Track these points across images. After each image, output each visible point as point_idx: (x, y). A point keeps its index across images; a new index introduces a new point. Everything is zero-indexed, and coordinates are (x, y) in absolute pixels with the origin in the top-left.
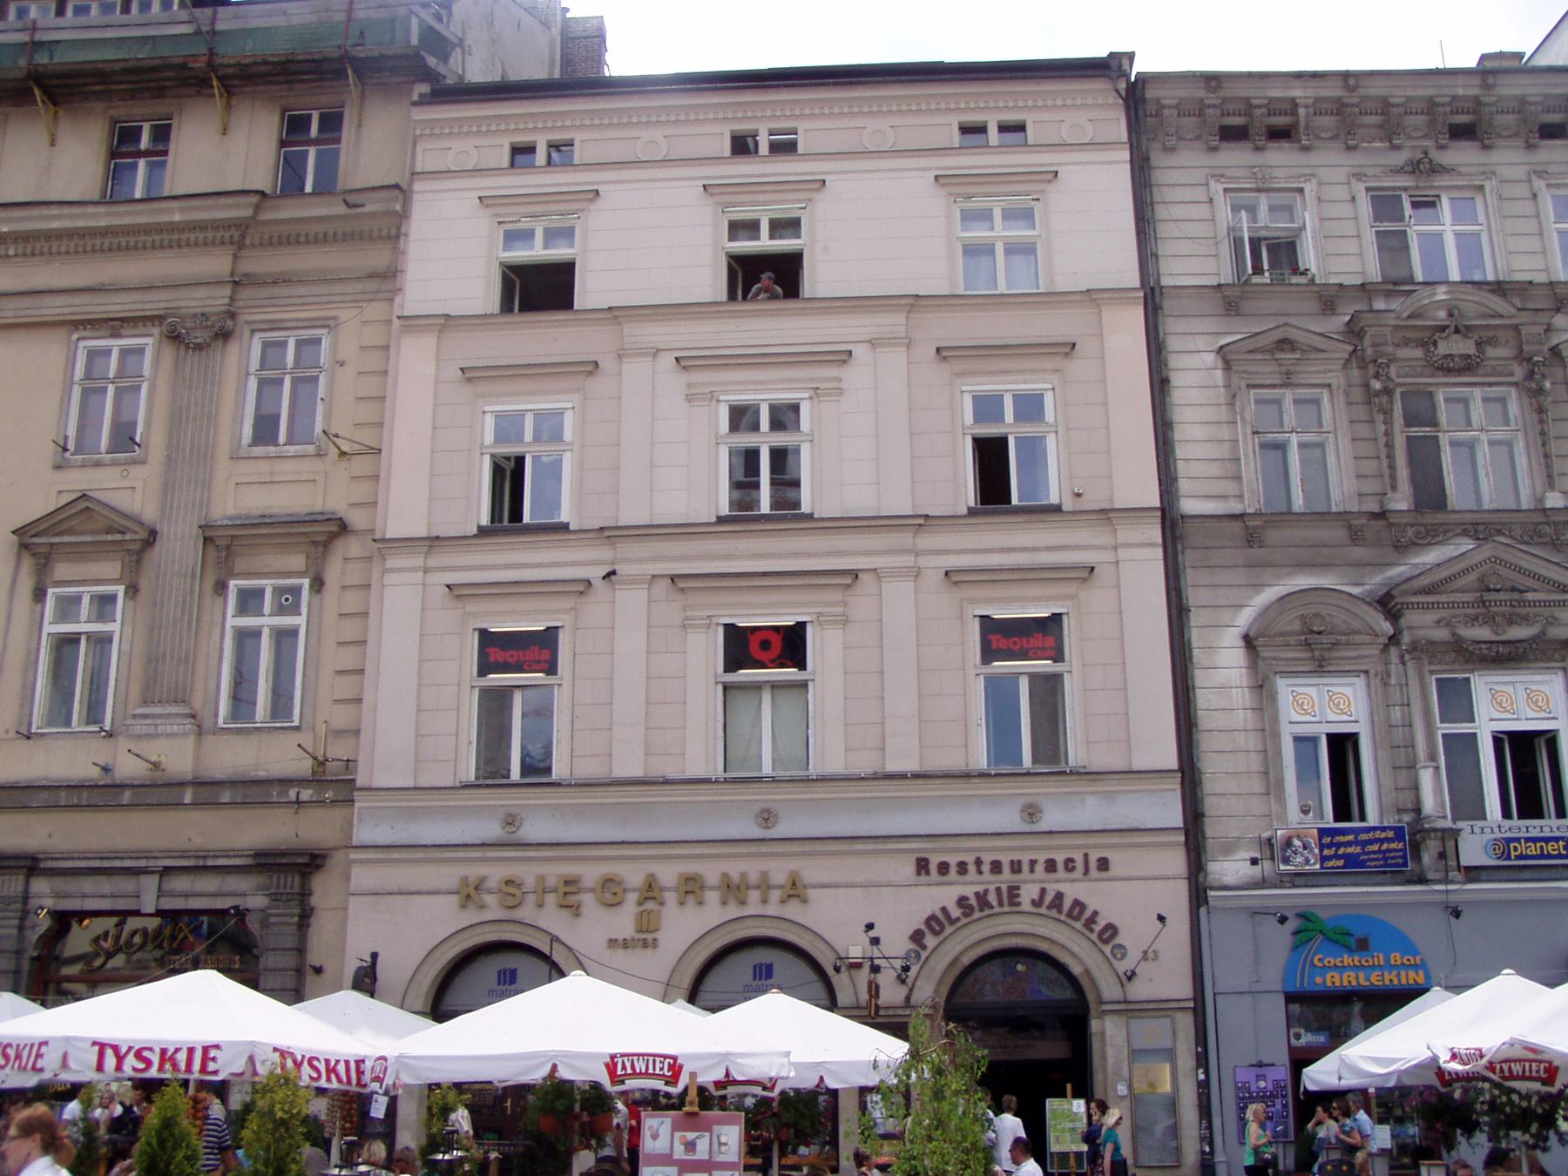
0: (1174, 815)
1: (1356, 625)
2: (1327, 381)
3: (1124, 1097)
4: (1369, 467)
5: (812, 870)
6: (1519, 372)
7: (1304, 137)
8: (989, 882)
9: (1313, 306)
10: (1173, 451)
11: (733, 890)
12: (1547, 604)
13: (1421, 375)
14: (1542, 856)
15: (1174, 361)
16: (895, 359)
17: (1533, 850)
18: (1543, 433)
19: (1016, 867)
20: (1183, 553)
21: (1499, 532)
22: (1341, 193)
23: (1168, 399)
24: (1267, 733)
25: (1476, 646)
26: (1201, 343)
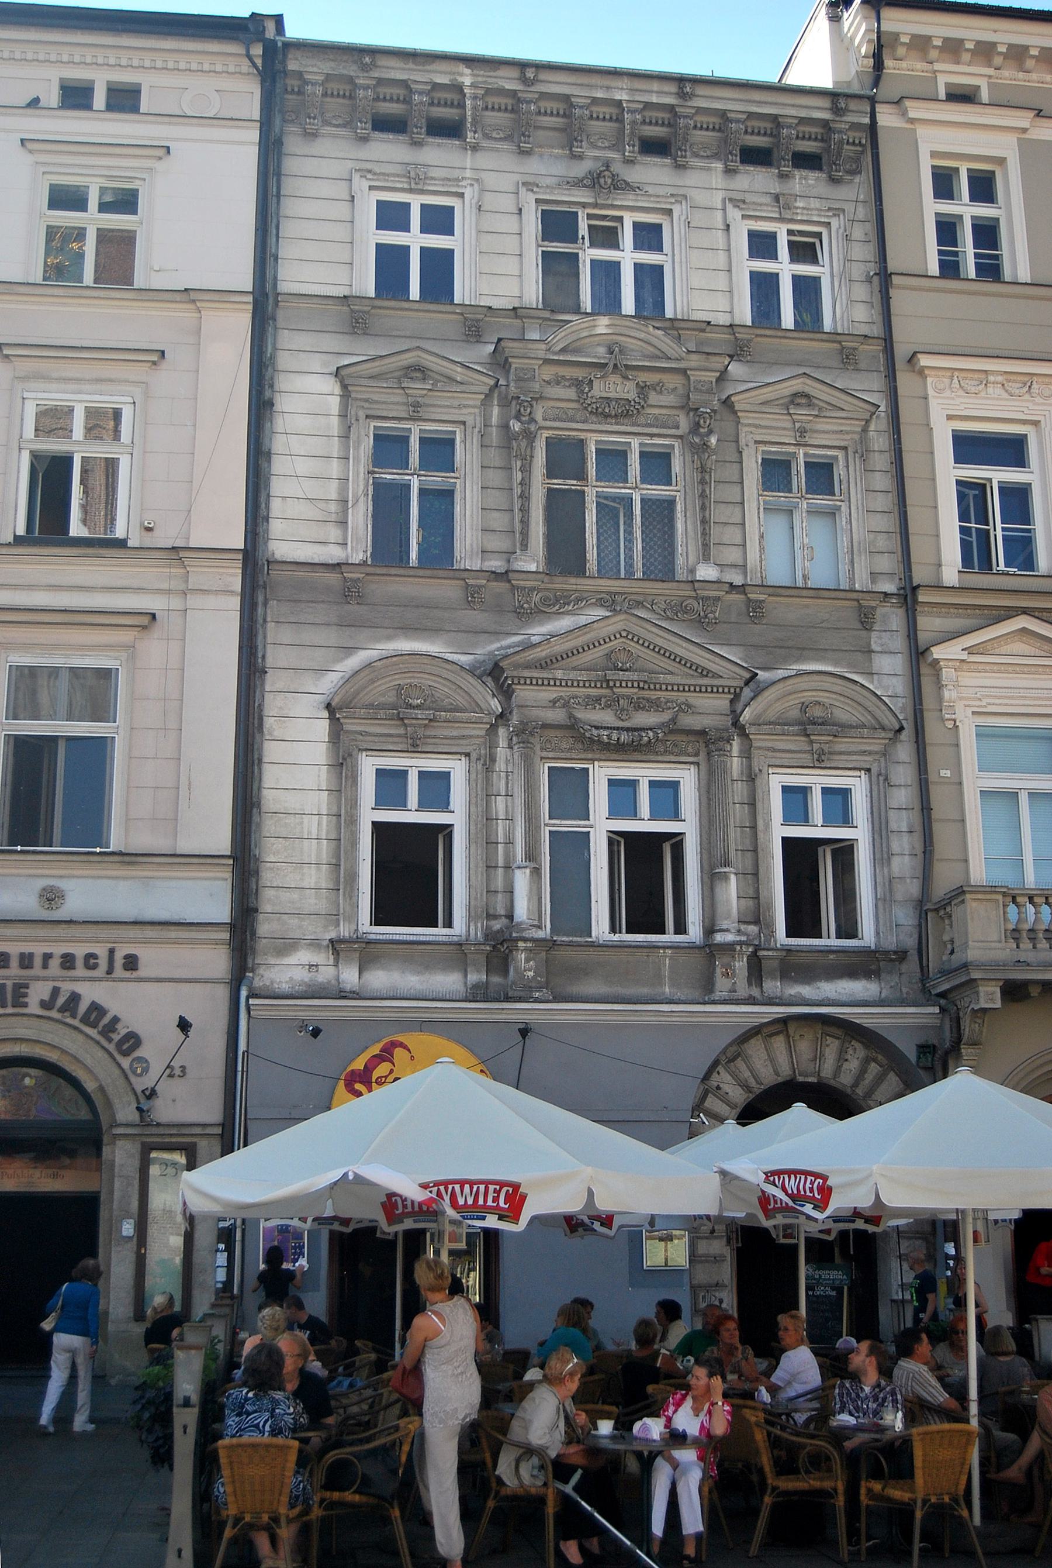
1: (461, 700)
2: (461, 419)
3: (130, 1238)
4: (499, 521)
6: (684, 423)
7: (470, 134)
10: (268, 486)
12: (681, 688)
15: (283, 382)
18: (703, 495)
20: (265, 604)
21: (639, 604)
22: (507, 203)
23: (268, 425)
24: (343, 818)
25: (595, 732)
26: (316, 363)
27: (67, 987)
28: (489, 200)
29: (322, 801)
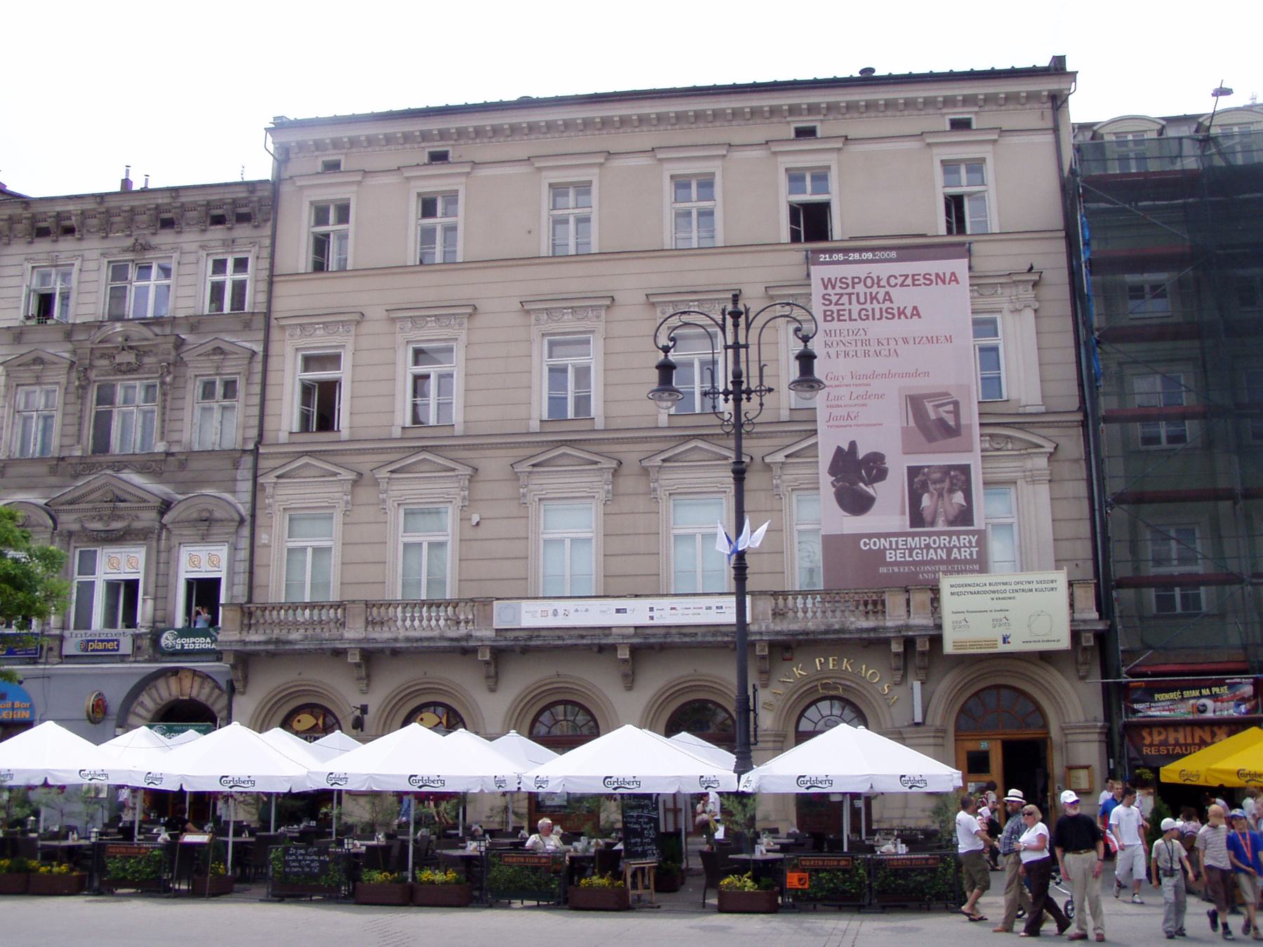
1: (41, 522)
9: (60, 336)
13: (109, 375)
14: (105, 650)
17: (101, 646)
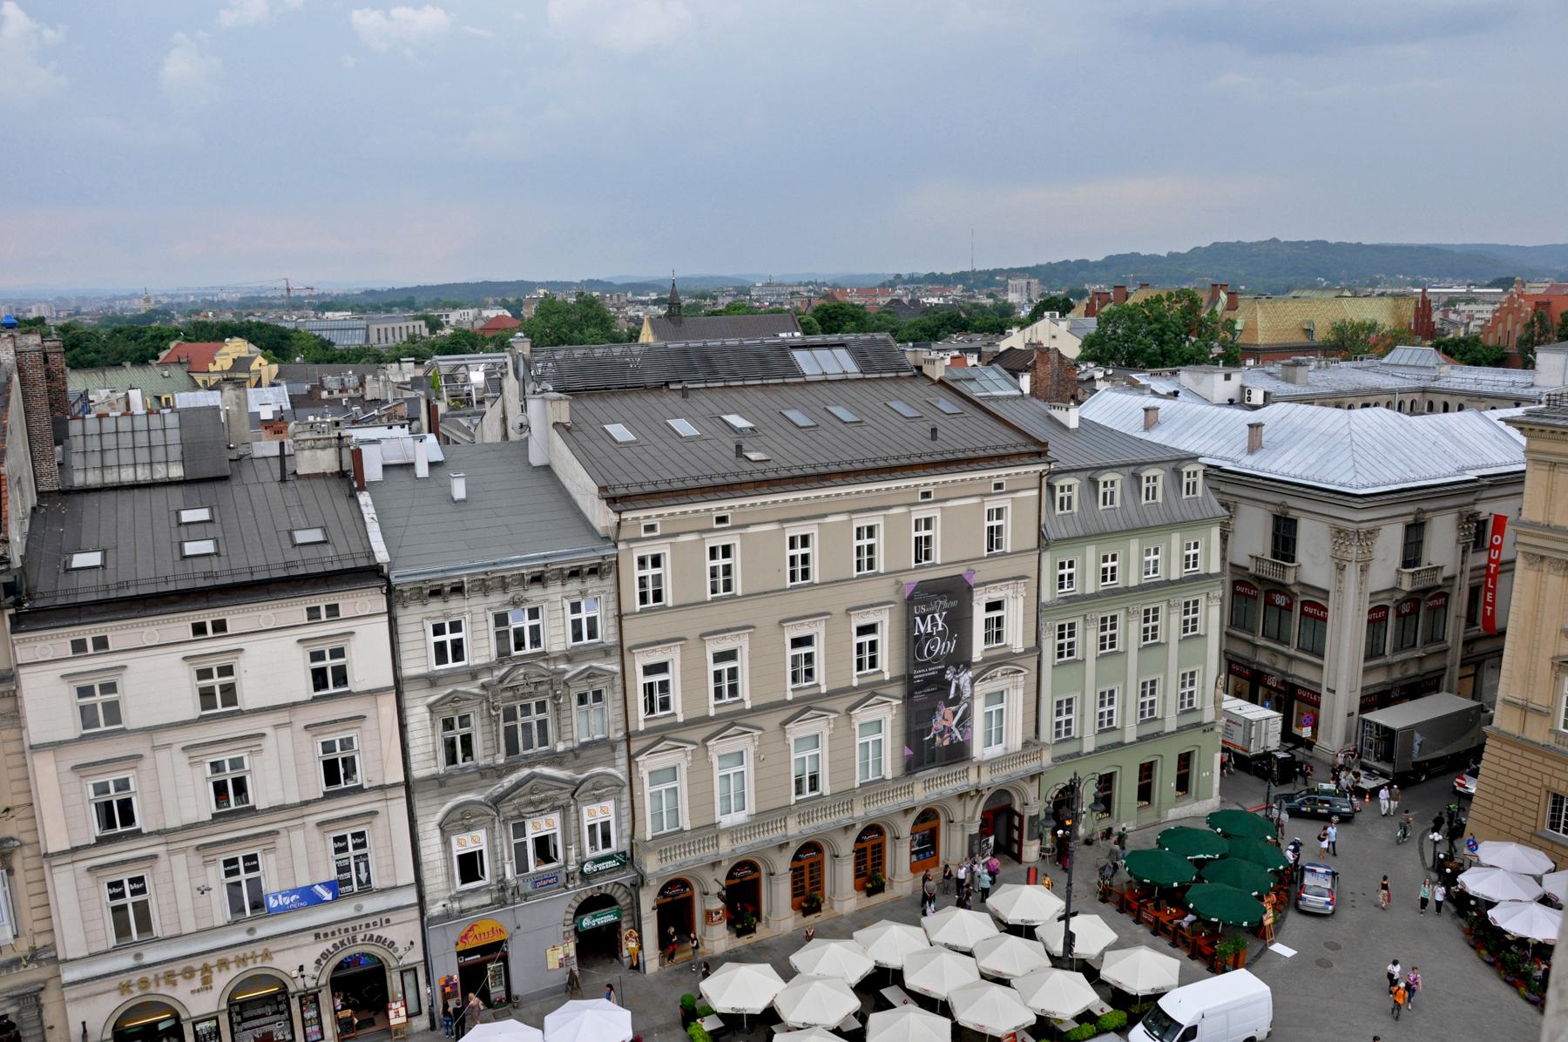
0: (414, 899)
5: (272, 946)
8: (344, 936)
11: (242, 961)
16: (286, 732)
19: (354, 929)
22: (482, 617)
26: (419, 702)
27: (368, 934)
28: (476, 618)
29: (441, 855)
